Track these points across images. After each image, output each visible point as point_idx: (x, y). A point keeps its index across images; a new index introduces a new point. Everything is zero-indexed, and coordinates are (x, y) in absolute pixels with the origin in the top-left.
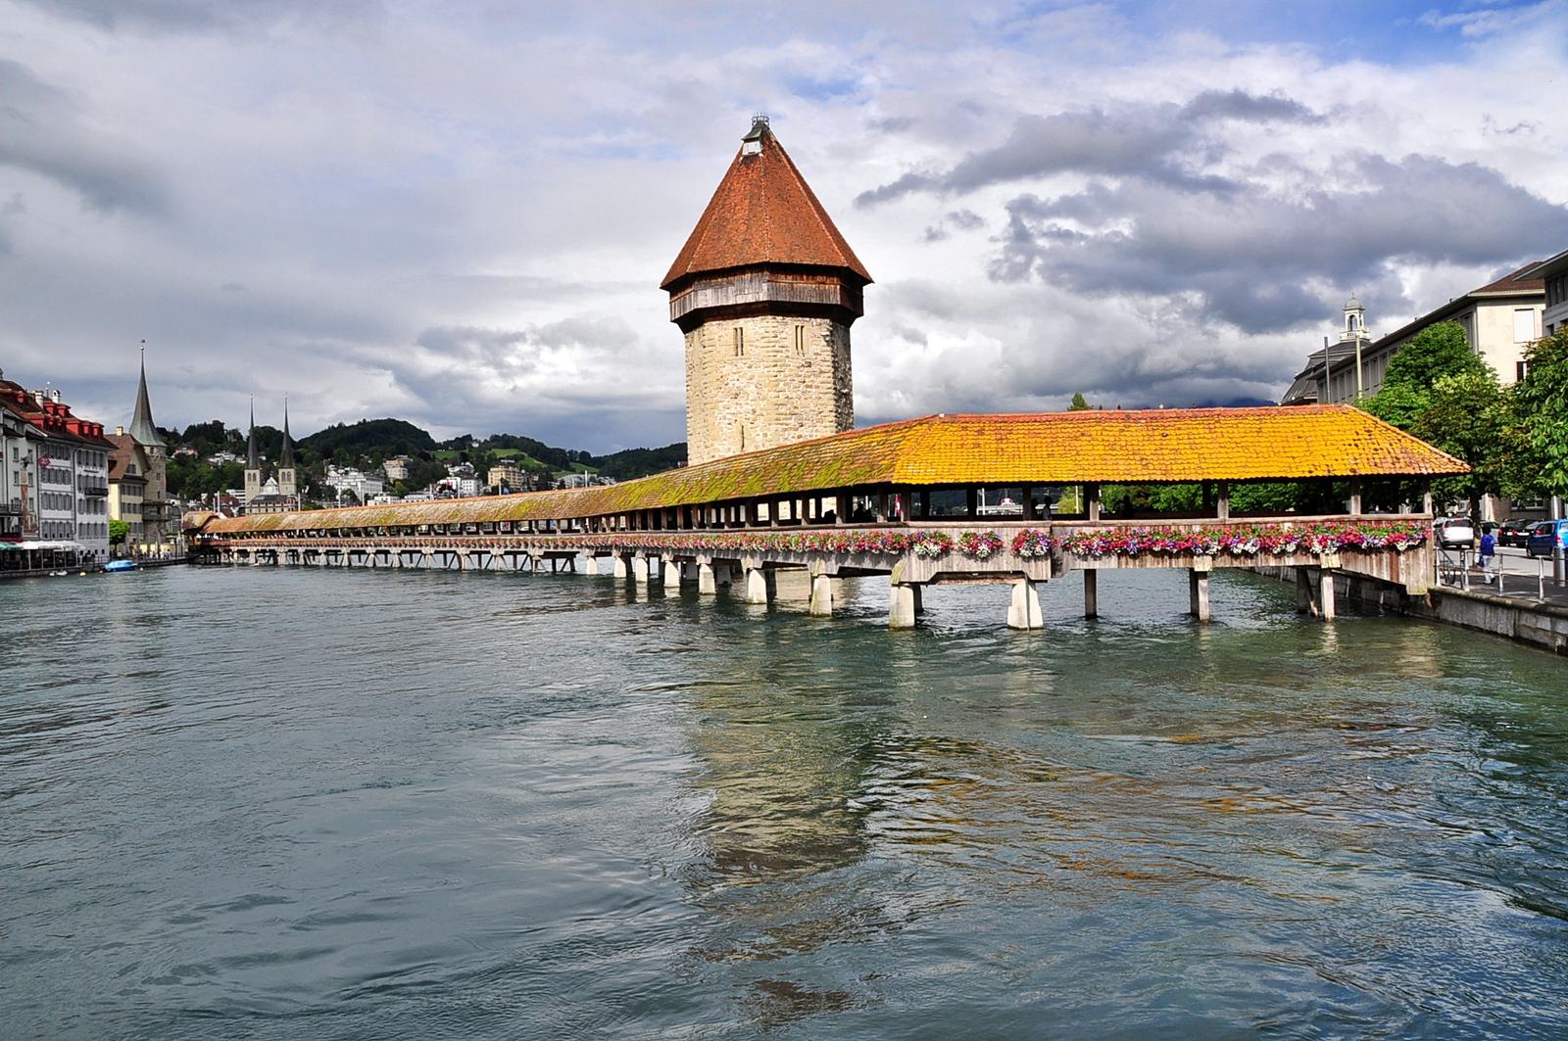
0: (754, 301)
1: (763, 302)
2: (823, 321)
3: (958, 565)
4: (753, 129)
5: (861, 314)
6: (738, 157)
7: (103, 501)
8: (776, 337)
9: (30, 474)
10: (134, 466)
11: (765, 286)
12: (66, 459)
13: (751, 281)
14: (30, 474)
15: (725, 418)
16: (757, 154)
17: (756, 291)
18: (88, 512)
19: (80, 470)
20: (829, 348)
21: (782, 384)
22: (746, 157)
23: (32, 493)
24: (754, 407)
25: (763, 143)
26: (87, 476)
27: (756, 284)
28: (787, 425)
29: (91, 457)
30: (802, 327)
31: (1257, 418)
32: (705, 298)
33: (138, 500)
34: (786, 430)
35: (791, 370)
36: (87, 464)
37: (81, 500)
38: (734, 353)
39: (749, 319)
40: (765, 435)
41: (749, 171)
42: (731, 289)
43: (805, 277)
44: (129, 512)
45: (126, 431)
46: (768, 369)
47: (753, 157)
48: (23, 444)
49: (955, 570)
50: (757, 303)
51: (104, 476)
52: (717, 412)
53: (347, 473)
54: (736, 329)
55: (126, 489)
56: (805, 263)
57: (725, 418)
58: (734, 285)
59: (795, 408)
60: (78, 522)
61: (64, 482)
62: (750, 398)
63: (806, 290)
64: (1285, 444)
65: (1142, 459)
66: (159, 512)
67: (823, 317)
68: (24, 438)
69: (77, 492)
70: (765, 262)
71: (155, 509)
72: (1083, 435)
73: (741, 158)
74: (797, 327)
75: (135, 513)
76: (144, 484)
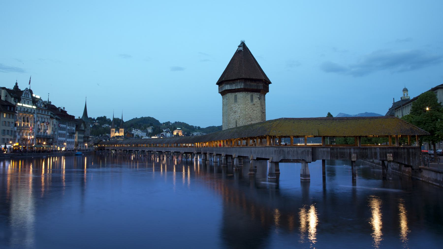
1: (242, 88)
3: (287, 158)
4: (241, 44)
5: (268, 92)
6: (237, 51)
7: (73, 136)
8: (246, 97)
9: (56, 128)
10: (82, 127)
11: (243, 84)
12: (65, 125)
13: (239, 83)
14: (56, 128)
15: (232, 118)
16: (242, 50)
17: (240, 86)
18: (70, 138)
19: (68, 128)
20: (259, 100)
21: (247, 110)
22: (239, 51)
23: (56, 133)
25: (243, 47)
26: (70, 129)
28: (248, 120)
29: (71, 124)
30: (253, 95)
31: (369, 119)
32: (227, 87)
33: (83, 136)
34: (248, 121)
35: (250, 106)
36: (70, 126)
37: (68, 135)
38: (234, 101)
40: (242, 123)
41: (240, 55)
42: (234, 85)
43: (253, 82)
44: (80, 139)
45: (81, 118)
46: (244, 106)
47: (241, 51)
48: (55, 121)
49: (286, 159)
50: (241, 88)
51: (74, 129)
52: (230, 116)
53: (137, 130)
54: (235, 95)
55: (80, 133)
56: (253, 78)
57: (232, 118)
58: (235, 84)
59: (250, 116)
60: (67, 141)
61: (64, 131)
62: (239, 113)
63: (254, 85)
64: (377, 127)
65: (337, 130)
66: (88, 139)
68: (55, 119)
69: (67, 133)
70: (243, 78)
71: (87, 138)
72: (321, 123)
73: (238, 51)
74: (251, 95)
75: (82, 139)
76: (84, 132)
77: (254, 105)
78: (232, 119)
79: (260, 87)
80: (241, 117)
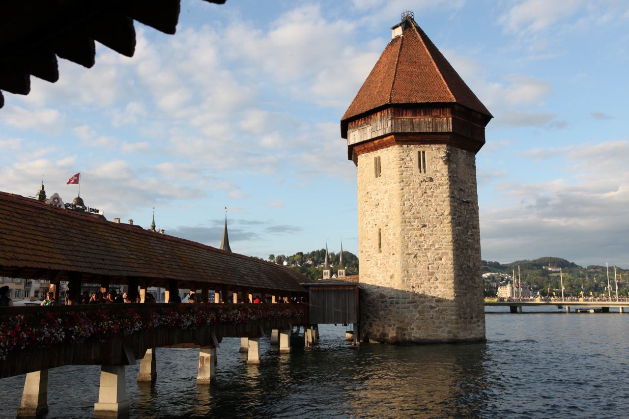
0: (382, 134)
2: (441, 146)
13: (381, 120)
24: (387, 214)
27: (384, 121)
30: (424, 152)
32: (356, 136)
39: (384, 149)
40: (394, 235)
41: (393, 48)
42: (369, 128)
47: (398, 38)
52: (364, 219)
59: (418, 213)
62: (385, 207)
63: (423, 123)
67: (441, 143)
74: (419, 153)
77: (431, 180)
78: (370, 226)
79: (445, 126)
80: (390, 217)
